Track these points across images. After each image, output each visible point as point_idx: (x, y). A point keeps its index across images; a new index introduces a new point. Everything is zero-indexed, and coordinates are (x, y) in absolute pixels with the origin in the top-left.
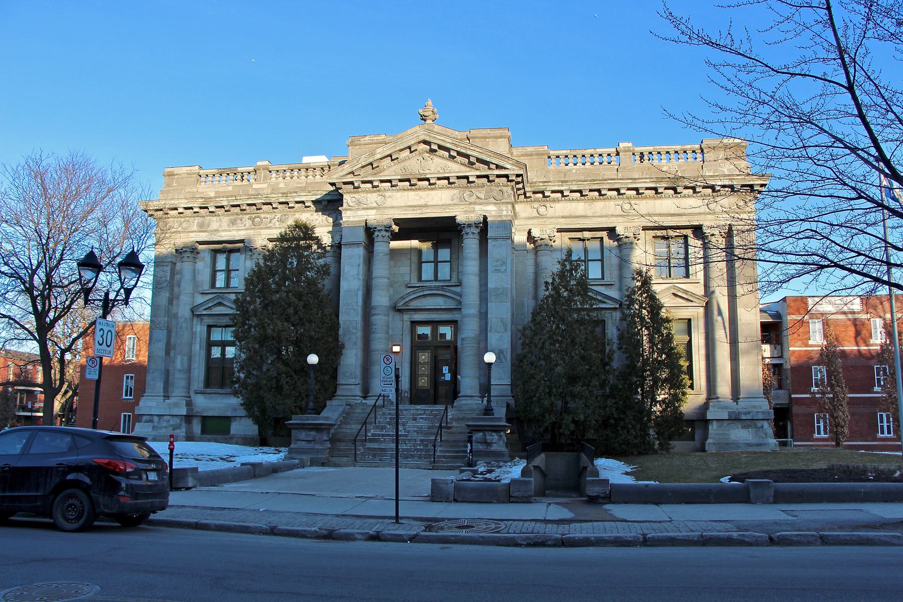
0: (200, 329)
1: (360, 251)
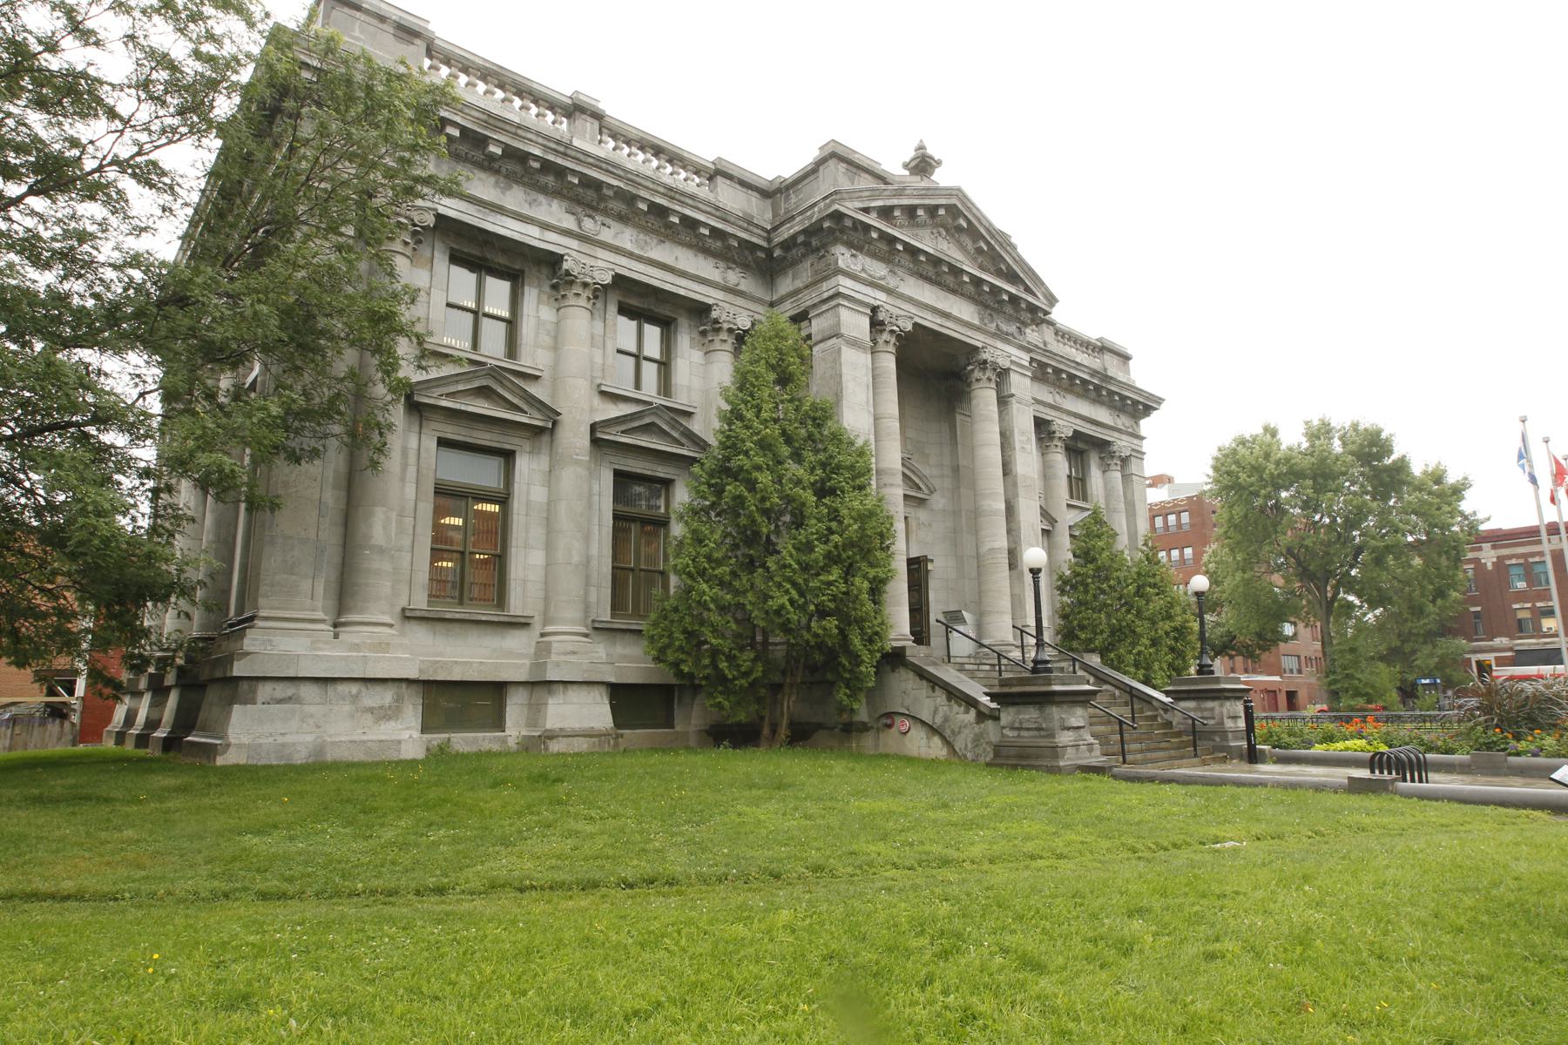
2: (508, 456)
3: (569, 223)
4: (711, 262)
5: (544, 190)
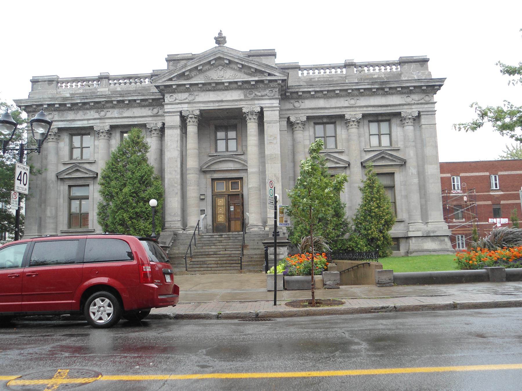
0: (64, 188)
1: (178, 132)
2: (88, 185)
3: (97, 116)
4: (147, 108)
5: (87, 109)
